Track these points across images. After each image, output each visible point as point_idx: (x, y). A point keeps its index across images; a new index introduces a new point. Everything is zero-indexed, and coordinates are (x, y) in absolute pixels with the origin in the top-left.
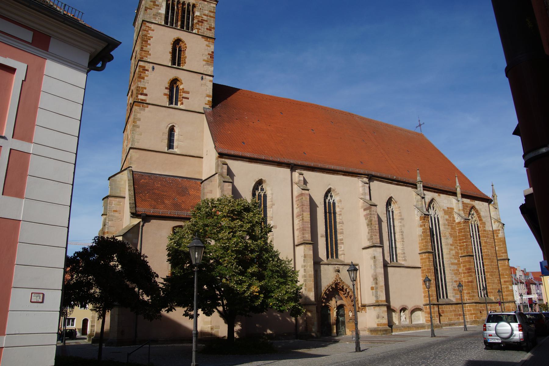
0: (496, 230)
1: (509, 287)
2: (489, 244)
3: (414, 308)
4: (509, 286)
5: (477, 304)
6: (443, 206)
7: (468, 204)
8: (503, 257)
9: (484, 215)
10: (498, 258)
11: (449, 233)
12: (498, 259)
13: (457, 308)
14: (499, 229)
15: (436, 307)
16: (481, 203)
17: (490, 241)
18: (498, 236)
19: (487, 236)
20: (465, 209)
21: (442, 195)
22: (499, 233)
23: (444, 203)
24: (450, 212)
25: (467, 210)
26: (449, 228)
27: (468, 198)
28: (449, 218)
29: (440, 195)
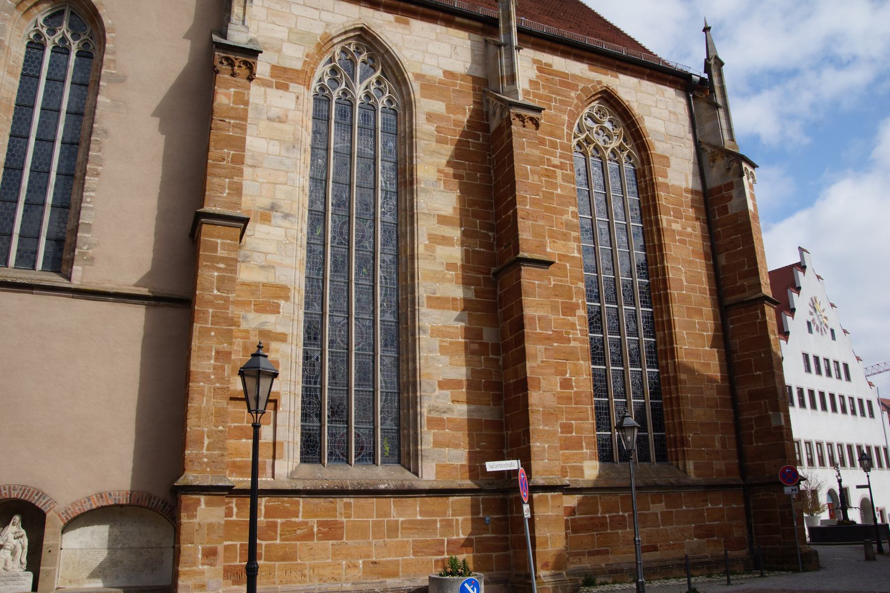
0: (719, 189)
1: (769, 416)
2: (682, 242)
3: (99, 504)
4: (771, 413)
5: (549, 494)
6: (423, 63)
7: (575, 77)
8: (744, 291)
9: (662, 130)
10: (730, 299)
11: (439, 171)
12: (726, 303)
13: (444, 513)
14: (729, 181)
15: (208, 504)
16: (648, 86)
17: (689, 230)
18: (725, 209)
19: (674, 209)
20: (559, 95)
21: (418, 26)
22: (730, 198)
23: (426, 52)
24: (459, 91)
25: (569, 97)
26: (443, 151)
27: (579, 58)
28: (447, 112)
29: (407, 23)
